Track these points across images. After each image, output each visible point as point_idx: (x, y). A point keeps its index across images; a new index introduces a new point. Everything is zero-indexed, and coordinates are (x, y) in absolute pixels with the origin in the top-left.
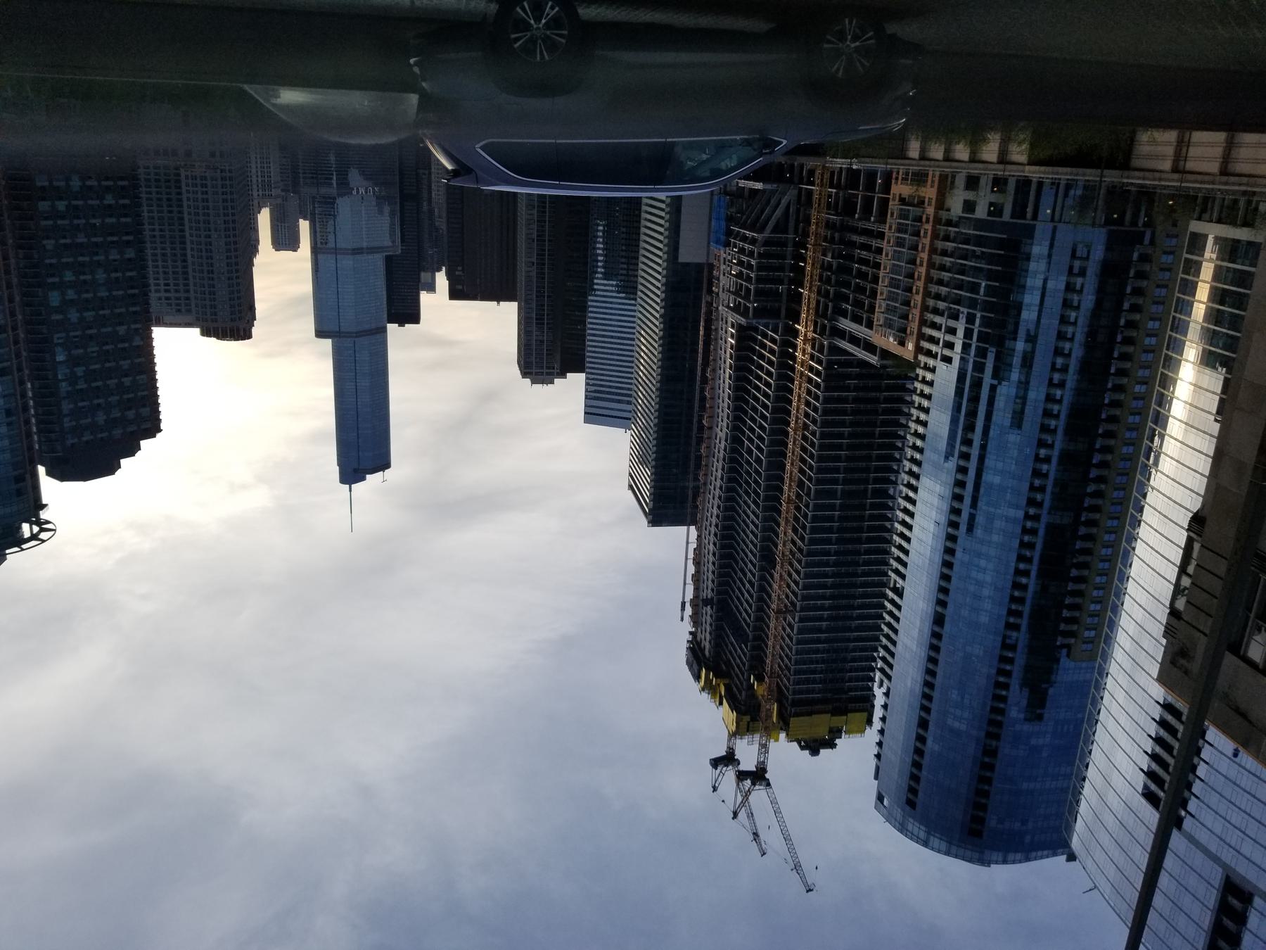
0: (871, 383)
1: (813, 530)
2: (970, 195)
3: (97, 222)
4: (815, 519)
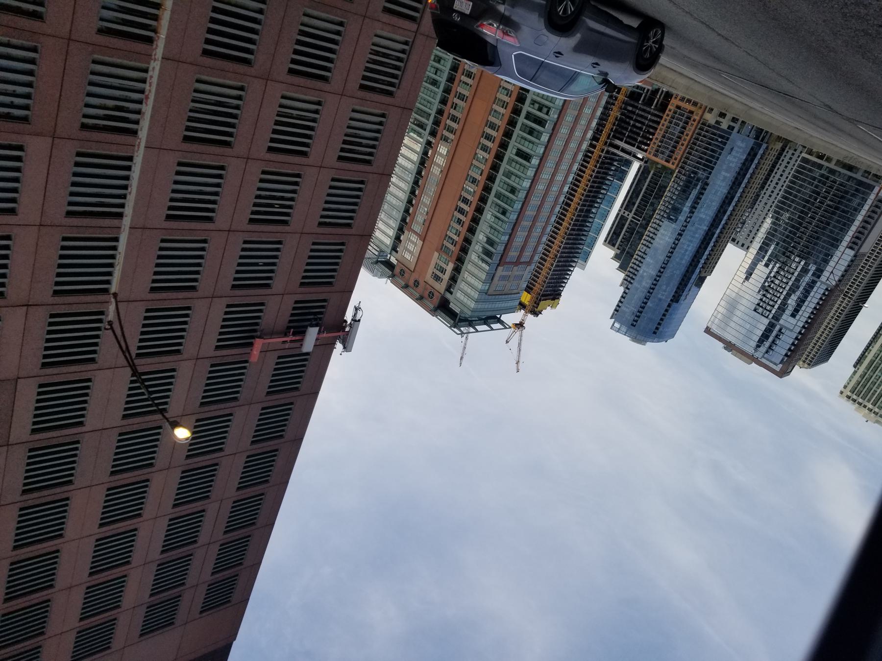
1: (574, 225)
2: (721, 120)
4: (576, 220)
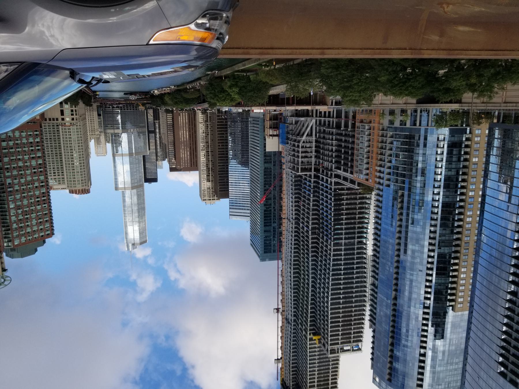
0: (352, 196)
3: (26, 149)
